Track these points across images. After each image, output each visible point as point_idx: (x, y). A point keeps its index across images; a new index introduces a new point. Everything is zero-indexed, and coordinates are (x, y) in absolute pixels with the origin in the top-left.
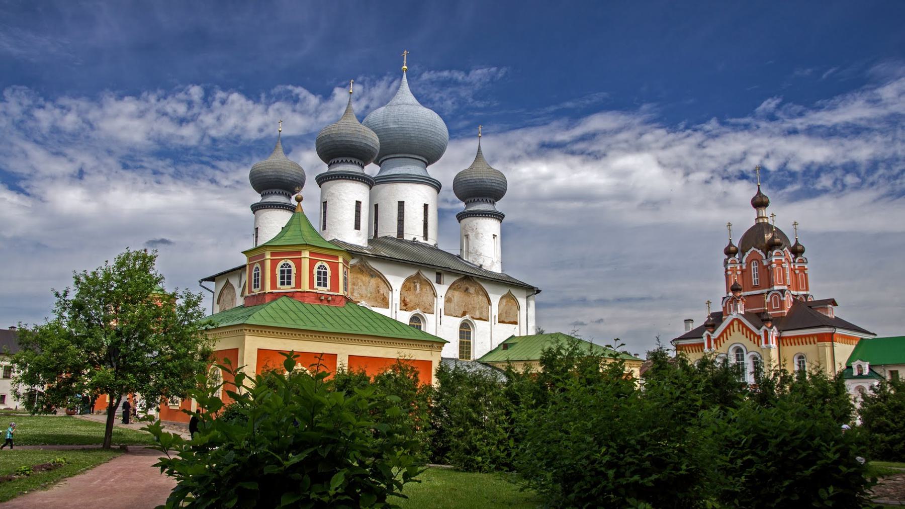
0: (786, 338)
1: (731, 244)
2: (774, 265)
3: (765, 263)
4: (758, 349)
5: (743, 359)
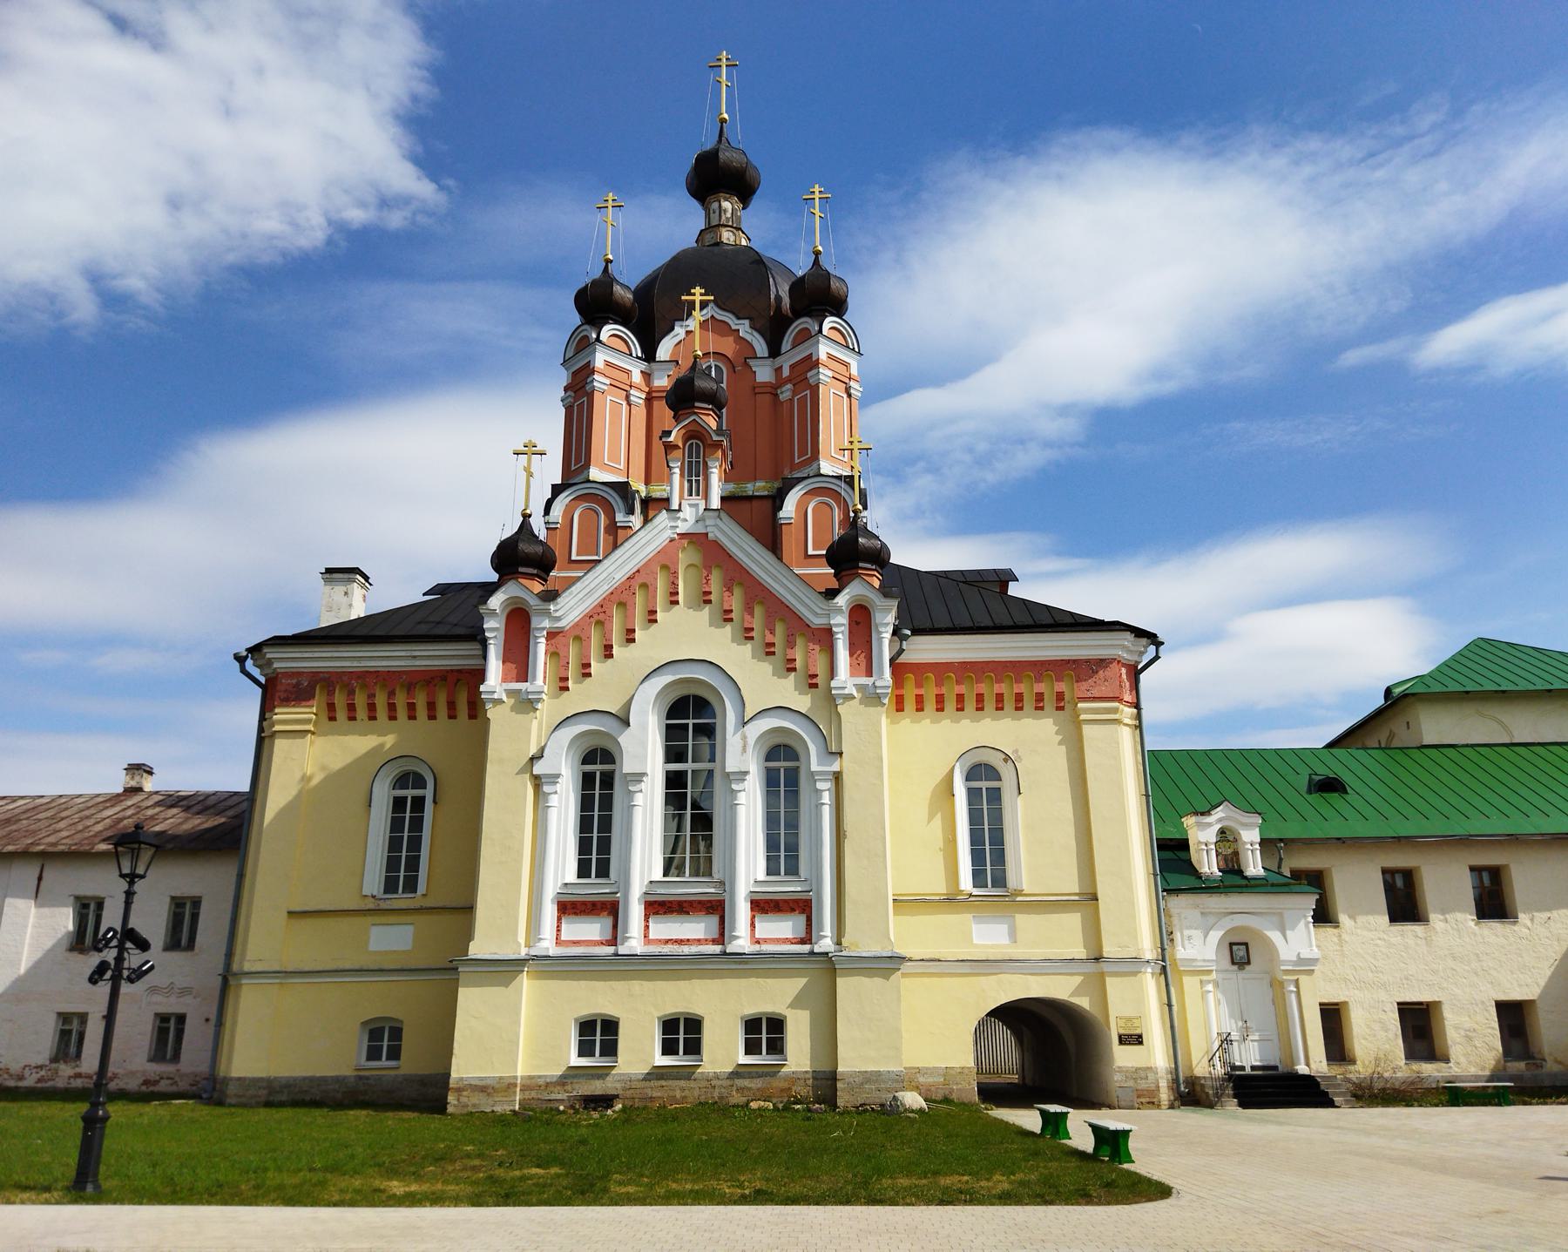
0: (920, 669)
2: (825, 374)
3: (764, 373)
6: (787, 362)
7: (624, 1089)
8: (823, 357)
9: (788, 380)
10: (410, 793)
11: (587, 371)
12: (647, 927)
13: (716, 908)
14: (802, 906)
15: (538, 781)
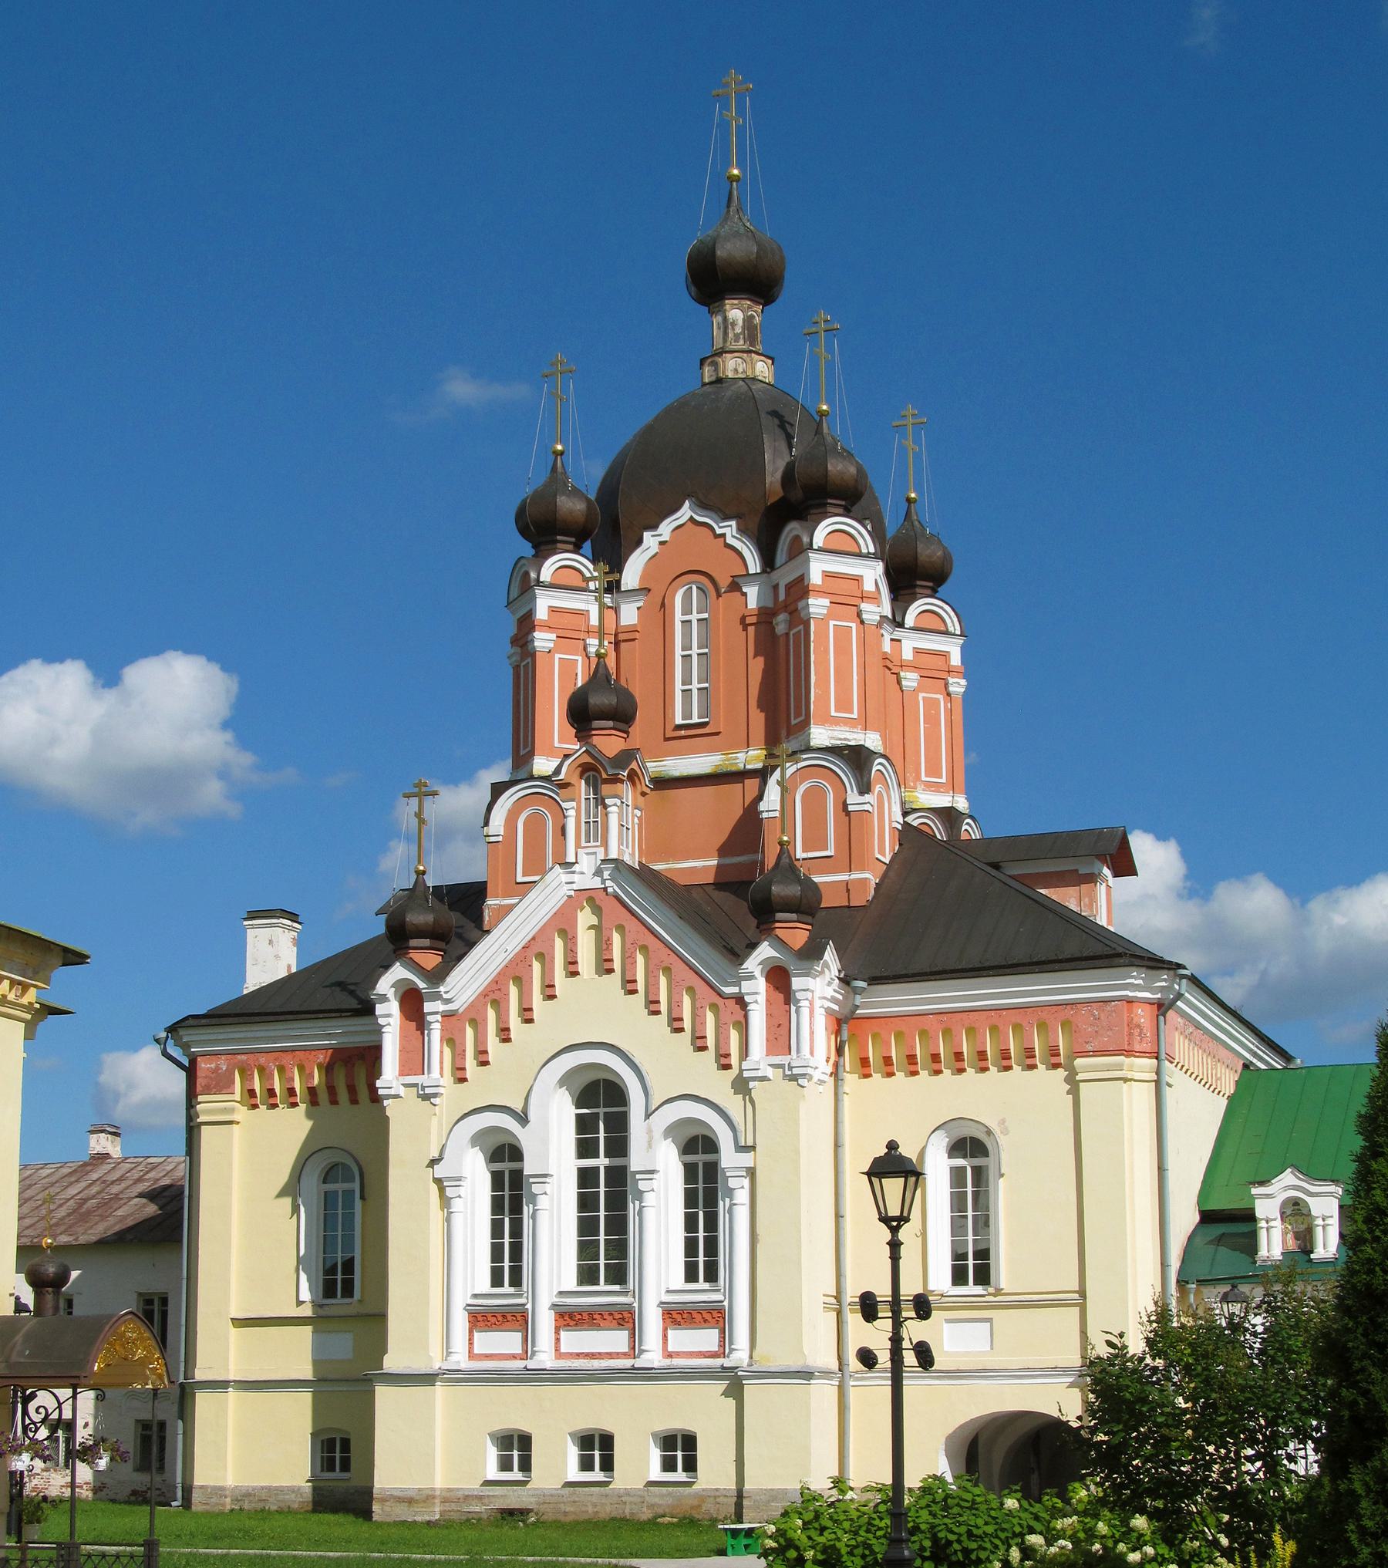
1: (556, 480)
2: (817, 606)
4: (719, 1087)
6: (784, 576)
7: (538, 1504)
8: (815, 577)
10: (339, 1187)
11: (527, 623)
12: (558, 1340)
13: (626, 1318)
14: (715, 1316)
15: (438, 1181)
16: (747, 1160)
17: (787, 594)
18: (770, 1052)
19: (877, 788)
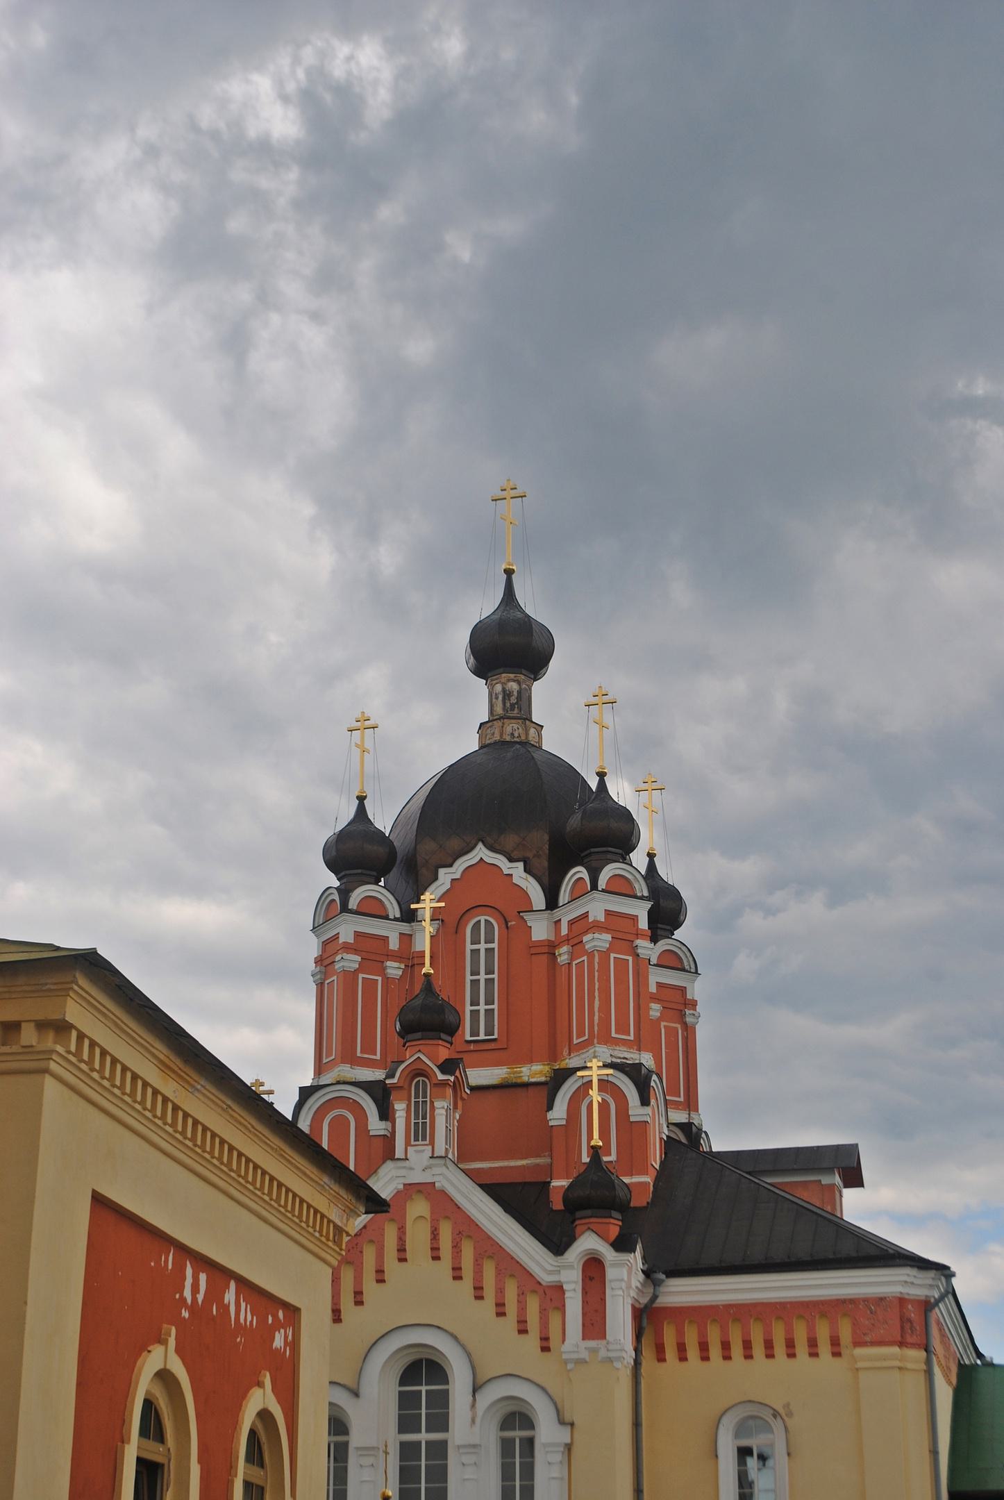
0: (681, 1314)
3: (540, 930)
5: (440, 1422)
6: (566, 915)
9: (567, 940)
16: (564, 1435)
17: (570, 929)
18: (585, 1337)
19: (653, 1102)
